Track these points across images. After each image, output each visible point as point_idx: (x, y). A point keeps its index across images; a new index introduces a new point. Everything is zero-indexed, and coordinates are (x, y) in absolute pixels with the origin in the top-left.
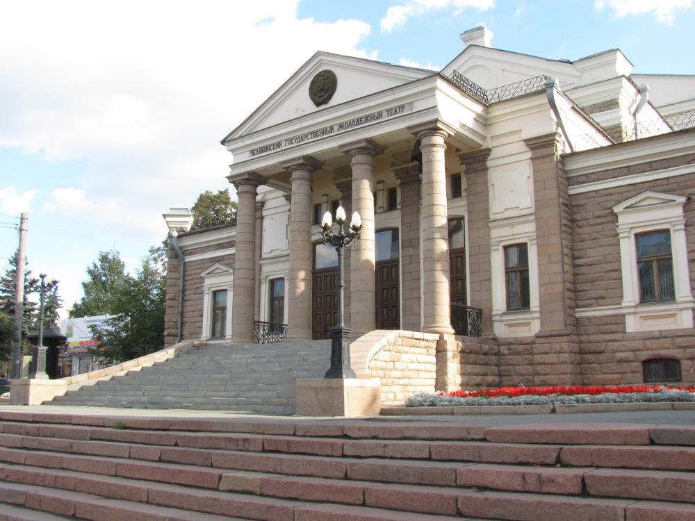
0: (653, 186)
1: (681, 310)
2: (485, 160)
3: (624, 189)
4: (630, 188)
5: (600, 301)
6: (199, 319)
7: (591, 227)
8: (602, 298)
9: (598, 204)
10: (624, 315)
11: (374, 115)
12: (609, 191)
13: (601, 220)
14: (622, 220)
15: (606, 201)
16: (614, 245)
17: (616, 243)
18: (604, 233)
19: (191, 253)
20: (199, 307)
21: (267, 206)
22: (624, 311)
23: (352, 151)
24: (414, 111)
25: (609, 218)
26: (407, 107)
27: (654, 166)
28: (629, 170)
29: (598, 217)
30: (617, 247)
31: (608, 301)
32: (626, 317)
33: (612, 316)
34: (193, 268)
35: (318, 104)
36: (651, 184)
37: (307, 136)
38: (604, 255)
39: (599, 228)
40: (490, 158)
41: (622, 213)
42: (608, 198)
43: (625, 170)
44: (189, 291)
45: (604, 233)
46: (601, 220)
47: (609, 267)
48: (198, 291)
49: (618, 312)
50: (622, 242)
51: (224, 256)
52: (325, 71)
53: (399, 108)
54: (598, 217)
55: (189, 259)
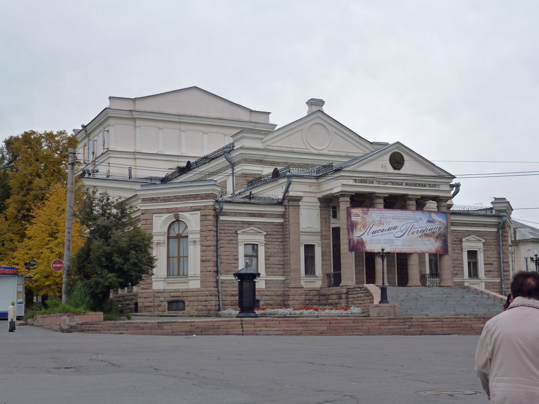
0: (473, 233)
1: (481, 282)
2: (423, 208)
3: (464, 232)
4: (466, 232)
5: (456, 276)
6: (236, 261)
7: (453, 245)
8: (457, 274)
9: (455, 236)
10: (464, 282)
11: (422, 184)
12: (459, 231)
13: (456, 243)
14: (464, 244)
15: (458, 235)
16: (460, 254)
17: (461, 252)
18: (457, 248)
19: (226, 214)
20: (235, 253)
21: (304, 199)
22: (465, 280)
23: (413, 199)
24: (440, 189)
25: (459, 242)
26: (437, 186)
27: (475, 225)
28: (466, 225)
29: (455, 241)
30: (461, 255)
31: (458, 276)
32: (465, 283)
33: (460, 282)
34: (225, 225)
35: (395, 168)
36: (473, 232)
37: (388, 183)
38: (457, 257)
39: (455, 246)
40: (425, 207)
41: (464, 241)
42: (458, 234)
43: (465, 224)
44: (223, 242)
45: (457, 248)
46: (456, 243)
47: (459, 262)
48: (232, 242)
49: (463, 281)
50: (463, 252)
51: (255, 222)
52: (396, 152)
53: (434, 185)
54: (455, 241)
55: (222, 218)
